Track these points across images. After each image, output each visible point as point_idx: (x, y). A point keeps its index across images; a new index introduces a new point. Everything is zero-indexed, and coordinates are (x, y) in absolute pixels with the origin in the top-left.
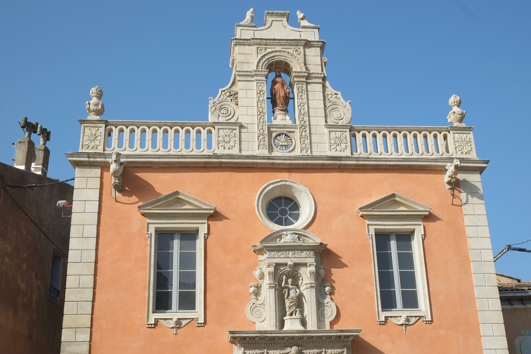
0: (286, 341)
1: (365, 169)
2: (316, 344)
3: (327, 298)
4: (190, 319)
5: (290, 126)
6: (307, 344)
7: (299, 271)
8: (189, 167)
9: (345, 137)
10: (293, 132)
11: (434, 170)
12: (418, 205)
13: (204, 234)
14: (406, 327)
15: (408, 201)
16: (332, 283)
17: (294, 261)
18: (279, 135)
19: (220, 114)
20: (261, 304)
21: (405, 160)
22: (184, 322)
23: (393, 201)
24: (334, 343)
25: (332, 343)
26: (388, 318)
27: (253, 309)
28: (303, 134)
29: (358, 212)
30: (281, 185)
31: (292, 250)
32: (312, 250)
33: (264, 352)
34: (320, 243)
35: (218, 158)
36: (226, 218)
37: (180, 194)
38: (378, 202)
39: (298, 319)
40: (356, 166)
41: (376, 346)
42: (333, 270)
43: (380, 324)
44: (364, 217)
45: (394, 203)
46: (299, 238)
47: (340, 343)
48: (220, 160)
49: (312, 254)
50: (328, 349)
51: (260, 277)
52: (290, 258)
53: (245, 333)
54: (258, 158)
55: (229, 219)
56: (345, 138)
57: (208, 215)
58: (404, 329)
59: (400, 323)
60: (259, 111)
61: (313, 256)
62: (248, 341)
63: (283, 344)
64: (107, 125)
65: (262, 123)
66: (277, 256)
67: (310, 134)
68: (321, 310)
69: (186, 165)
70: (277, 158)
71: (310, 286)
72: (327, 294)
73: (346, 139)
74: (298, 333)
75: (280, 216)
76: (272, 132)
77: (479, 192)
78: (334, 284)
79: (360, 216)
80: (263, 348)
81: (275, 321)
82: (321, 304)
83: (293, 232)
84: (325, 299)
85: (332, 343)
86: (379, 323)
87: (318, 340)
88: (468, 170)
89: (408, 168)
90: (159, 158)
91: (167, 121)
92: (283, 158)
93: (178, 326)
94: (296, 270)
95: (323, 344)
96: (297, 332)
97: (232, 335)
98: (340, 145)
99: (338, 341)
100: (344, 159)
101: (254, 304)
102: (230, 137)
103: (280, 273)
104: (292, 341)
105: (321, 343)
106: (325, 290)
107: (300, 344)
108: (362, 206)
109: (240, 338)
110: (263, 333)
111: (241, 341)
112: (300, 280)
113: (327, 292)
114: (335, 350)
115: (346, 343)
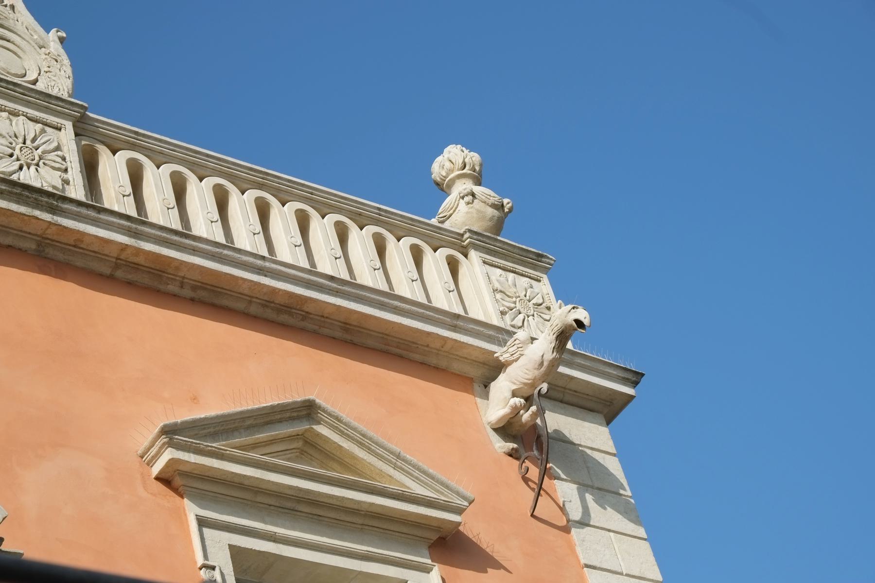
9: (55, 144)
11: (437, 368)
12: (416, 473)
15: (374, 447)
23: (299, 444)
29: (142, 457)
38: (243, 419)
40: (117, 266)
44: (178, 481)
45: (302, 452)
77: (622, 492)
79: (157, 478)
88: (561, 401)
89: (338, 334)
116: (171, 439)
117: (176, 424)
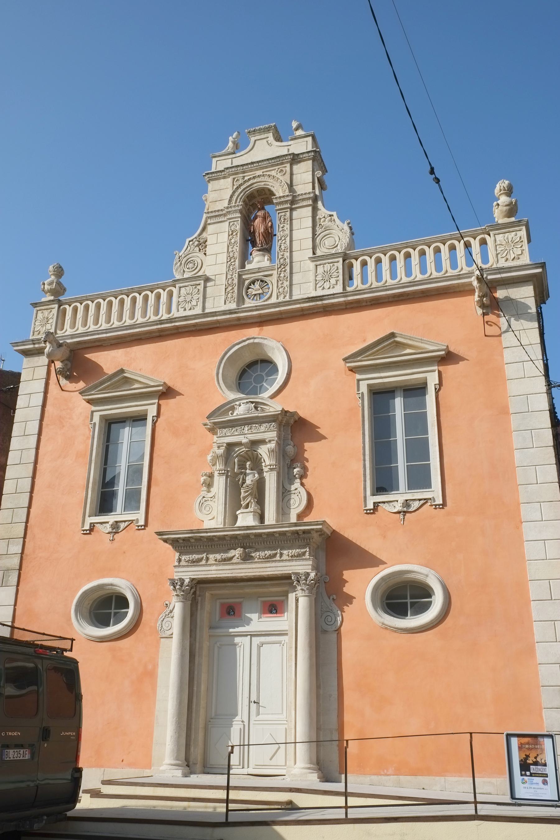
0: (229, 541)
1: (361, 307)
2: (268, 543)
3: (296, 483)
4: (130, 521)
5: (266, 268)
6: (257, 544)
7: (258, 451)
9: (336, 268)
10: (271, 275)
11: (460, 291)
12: (428, 343)
13: (153, 416)
14: (404, 515)
15: (414, 339)
16: (305, 462)
17: (250, 438)
18: (253, 282)
19: (186, 270)
20: (212, 498)
21: (412, 284)
22: (122, 526)
23: (395, 344)
24: (291, 542)
25: (288, 542)
26: (379, 504)
27: (203, 503)
28: (282, 275)
30: (248, 344)
31: (248, 424)
32: (274, 421)
33: (203, 557)
34: (281, 411)
36: (180, 394)
37: (126, 371)
38: (369, 347)
39: (251, 512)
40: (346, 305)
41: (358, 543)
42: (307, 445)
43: (366, 513)
44: (354, 370)
45: (396, 346)
46: (256, 408)
47: (300, 541)
48: (173, 324)
49: (273, 426)
50: (285, 550)
51: (212, 462)
52: (245, 434)
53: (174, 533)
54: (217, 314)
56: (335, 271)
57: (158, 393)
58: (401, 518)
59: (395, 510)
60: (229, 257)
61: (275, 428)
62: (182, 544)
63: (226, 546)
64: (61, 304)
65: (232, 271)
66: (229, 434)
67: (291, 273)
68: (286, 499)
69: (139, 337)
70: (240, 310)
71: (269, 469)
72: (296, 478)
73: (337, 271)
74: (239, 530)
75: (254, 384)
76: (245, 280)
77: (529, 311)
78: (307, 464)
80: (203, 553)
81: (223, 518)
82: (287, 491)
83: (248, 401)
84: (294, 484)
85: (288, 542)
86: (365, 512)
87: (269, 539)
88: (514, 283)
89: (421, 295)
90: (106, 333)
92: (248, 309)
93: (114, 530)
94: (255, 449)
95: (277, 543)
96: (238, 528)
97: (160, 537)
98: (329, 281)
99: (297, 538)
100: (327, 297)
101: (204, 497)
102: (193, 294)
103: (234, 456)
104: (237, 541)
105: (274, 543)
106: (294, 473)
107: (248, 545)
108: (346, 355)
109: (173, 541)
110: (195, 532)
111: (174, 545)
112: (263, 463)
113: (296, 475)
114: (295, 550)
115: (308, 541)
116: (346, 361)
117: (346, 357)
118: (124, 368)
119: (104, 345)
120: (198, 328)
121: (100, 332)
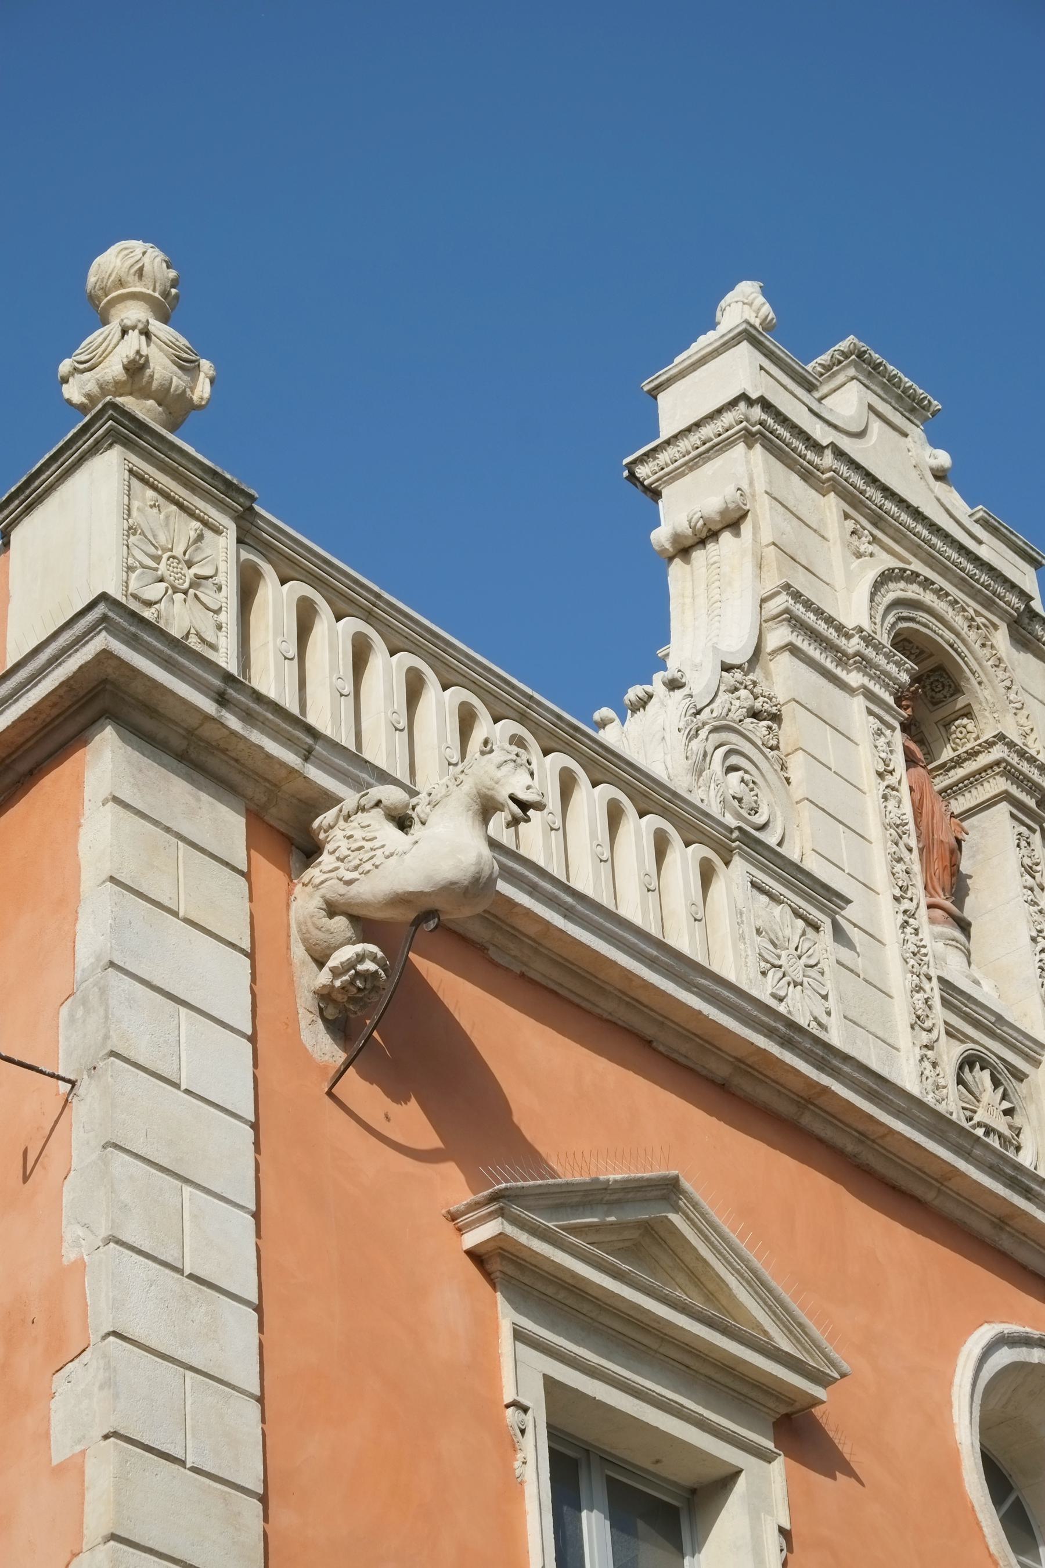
5: (1015, 1035)
8: (655, 1050)
35: (821, 1065)
48: (825, 1080)
54: (978, 1152)
55: (863, 1485)
69: (649, 1031)
90: (568, 913)
91: (537, 696)
118: (686, 1184)
119: (493, 953)
120: (869, 1158)
121: (548, 886)
